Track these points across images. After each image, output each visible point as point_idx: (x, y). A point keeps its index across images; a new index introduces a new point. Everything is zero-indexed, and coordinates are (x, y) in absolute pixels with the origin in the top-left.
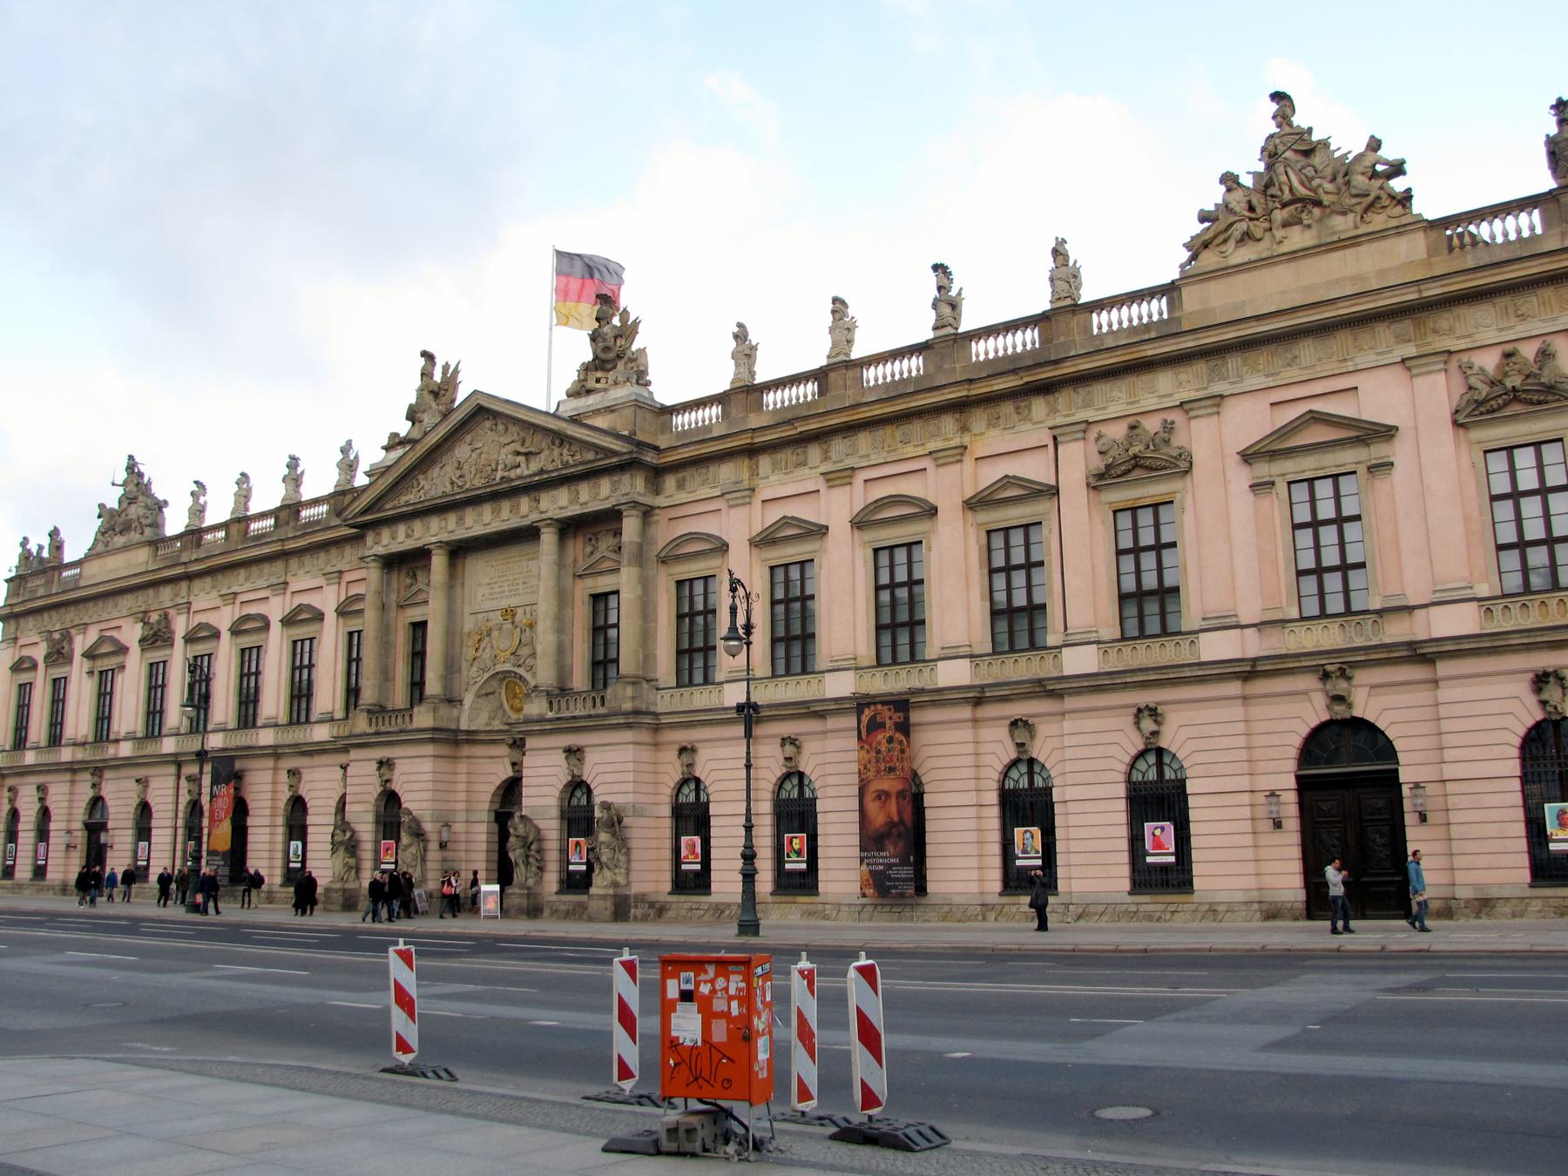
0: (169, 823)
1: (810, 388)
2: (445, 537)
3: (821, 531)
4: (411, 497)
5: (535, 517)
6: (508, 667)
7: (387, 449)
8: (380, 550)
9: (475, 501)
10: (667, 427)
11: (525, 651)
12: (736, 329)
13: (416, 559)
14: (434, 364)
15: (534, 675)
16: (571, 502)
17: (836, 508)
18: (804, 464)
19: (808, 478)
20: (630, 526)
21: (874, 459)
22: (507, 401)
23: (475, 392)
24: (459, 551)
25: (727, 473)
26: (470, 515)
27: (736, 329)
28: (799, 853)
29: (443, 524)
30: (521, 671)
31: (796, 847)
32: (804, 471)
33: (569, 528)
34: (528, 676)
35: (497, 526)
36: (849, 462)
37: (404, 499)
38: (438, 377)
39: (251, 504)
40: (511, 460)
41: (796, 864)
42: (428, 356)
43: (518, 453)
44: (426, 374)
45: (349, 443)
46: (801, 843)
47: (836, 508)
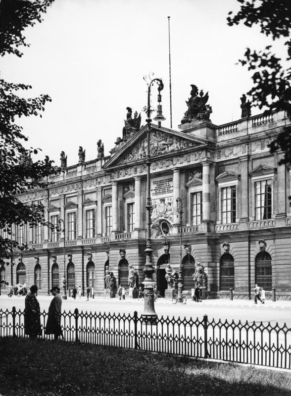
0: (63, 270)
4: (128, 161)
5: (171, 167)
6: (163, 218)
7: (117, 143)
11: (169, 213)
12: (242, 96)
13: (131, 182)
14: (131, 112)
15: (172, 221)
24: (143, 179)
27: (242, 96)
30: (168, 220)
34: (170, 222)
38: (133, 117)
39: (67, 164)
40: (162, 147)
42: (129, 109)
43: (165, 144)
44: (129, 116)
45: (100, 141)
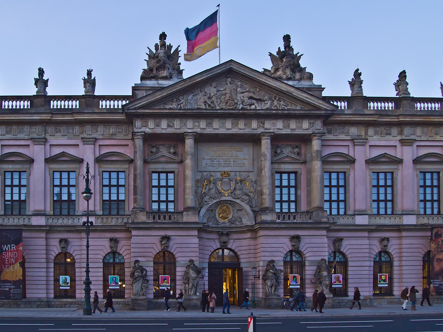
1: (391, 105)
2: (199, 131)
3: (400, 161)
5: (260, 130)
8: (147, 130)
9: (223, 116)
10: (366, 107)
16: (259, 127)
17: (407, 154)
18: (390, 134)
19: (393, 139)
20: (316, 144)
21: (423, 138)
22: (255, 70)
23: (231, 60)
24: (201, 139)
25: (354, 131)
26: (216, 124)
28: (385, 281)
29: (197, 124)
31: (383, 279)
32: (390, 137)
33: (277, 140)
35: (235, 131)
36: (412, 137)
37: (167, 107)
41: (383, 285)
43: (251, 98)
46: (386, 276)
47: (407, 154)
